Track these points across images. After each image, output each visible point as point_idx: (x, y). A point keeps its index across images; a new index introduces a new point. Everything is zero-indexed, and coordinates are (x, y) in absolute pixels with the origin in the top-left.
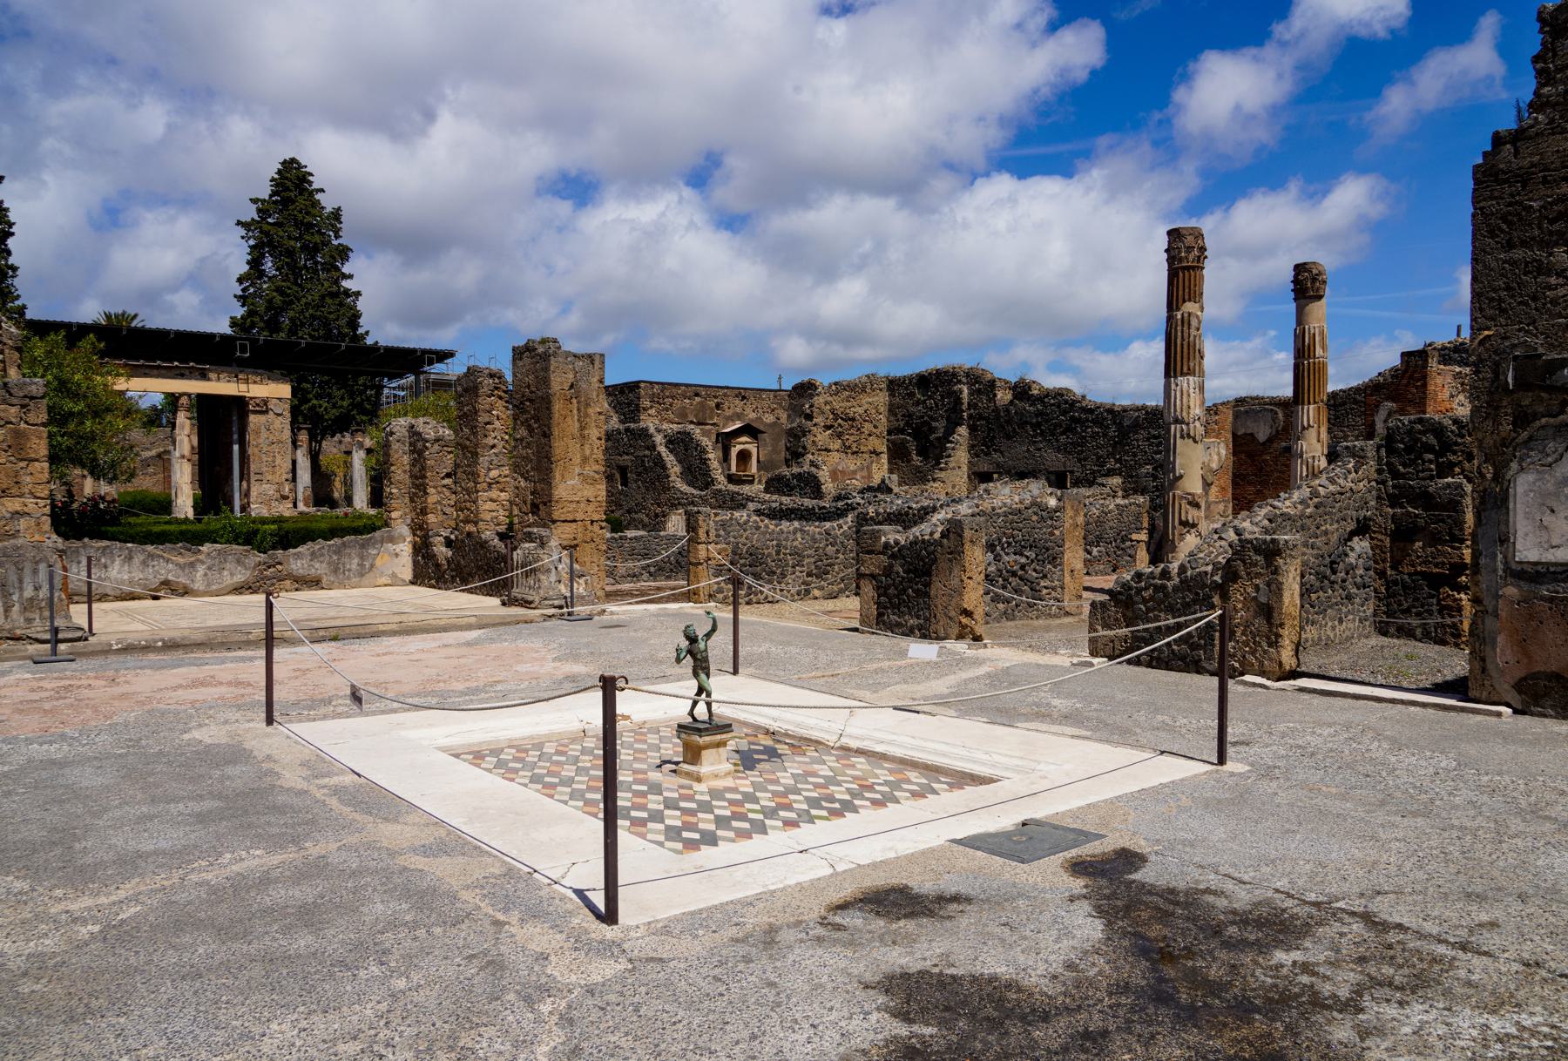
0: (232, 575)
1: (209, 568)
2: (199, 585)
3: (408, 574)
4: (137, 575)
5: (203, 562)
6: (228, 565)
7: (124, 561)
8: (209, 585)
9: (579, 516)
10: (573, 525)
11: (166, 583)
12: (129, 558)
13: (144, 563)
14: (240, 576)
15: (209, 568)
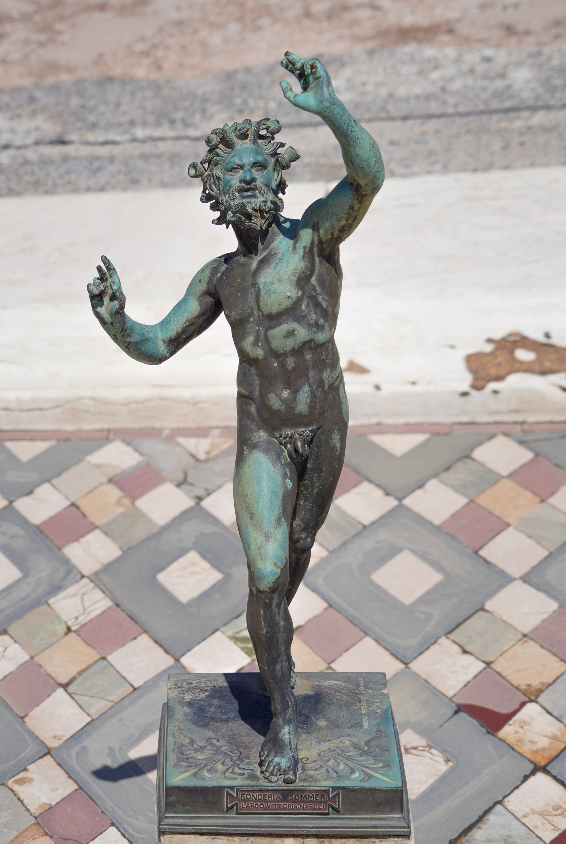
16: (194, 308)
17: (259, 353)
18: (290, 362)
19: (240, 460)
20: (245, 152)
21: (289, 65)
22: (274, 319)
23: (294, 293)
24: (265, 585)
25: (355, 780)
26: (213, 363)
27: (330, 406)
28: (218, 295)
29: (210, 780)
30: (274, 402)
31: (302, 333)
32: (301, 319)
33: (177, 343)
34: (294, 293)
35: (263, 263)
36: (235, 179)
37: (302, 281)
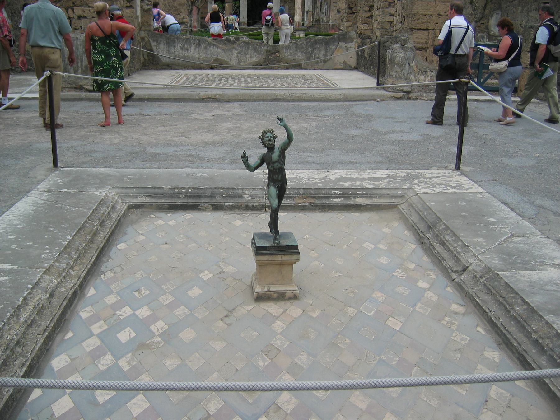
0: (251, 57)
1: (239, 53)
2: (234, 62)
3: (353, 62)
4: (203, 55)
5: (236, 49)
6: (250, 52)
7: (196, 46)
8: (239, 63)
9: (431, 26)
10: (426, 33)
11: (216, 60)
12: (199, 45)
13: (205, 48)
14: (256, 59)
15: (239, 53)
16: (259, 161)
17: (272, 169)
18: (277, 170)
19: (268, 188)
20: (269, 135)
21: (278, 118)
22: (274, 163)
23: (278, 158)
24: (274, 209)
25: (290, 244)
26: (262, 173)
27: (284, 180)
28: (263, 160)
29: (264, 245)
30: (274, 177)
31: (280, 165)
32: (280, 163)
33: (256, 168)
34: (278, 158)
35: (272, 153)
36: (267, 139)
37: (279, 156)
